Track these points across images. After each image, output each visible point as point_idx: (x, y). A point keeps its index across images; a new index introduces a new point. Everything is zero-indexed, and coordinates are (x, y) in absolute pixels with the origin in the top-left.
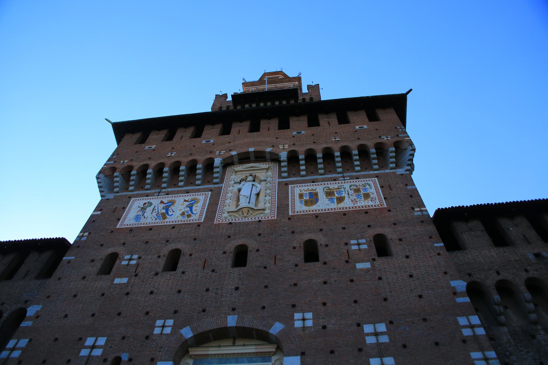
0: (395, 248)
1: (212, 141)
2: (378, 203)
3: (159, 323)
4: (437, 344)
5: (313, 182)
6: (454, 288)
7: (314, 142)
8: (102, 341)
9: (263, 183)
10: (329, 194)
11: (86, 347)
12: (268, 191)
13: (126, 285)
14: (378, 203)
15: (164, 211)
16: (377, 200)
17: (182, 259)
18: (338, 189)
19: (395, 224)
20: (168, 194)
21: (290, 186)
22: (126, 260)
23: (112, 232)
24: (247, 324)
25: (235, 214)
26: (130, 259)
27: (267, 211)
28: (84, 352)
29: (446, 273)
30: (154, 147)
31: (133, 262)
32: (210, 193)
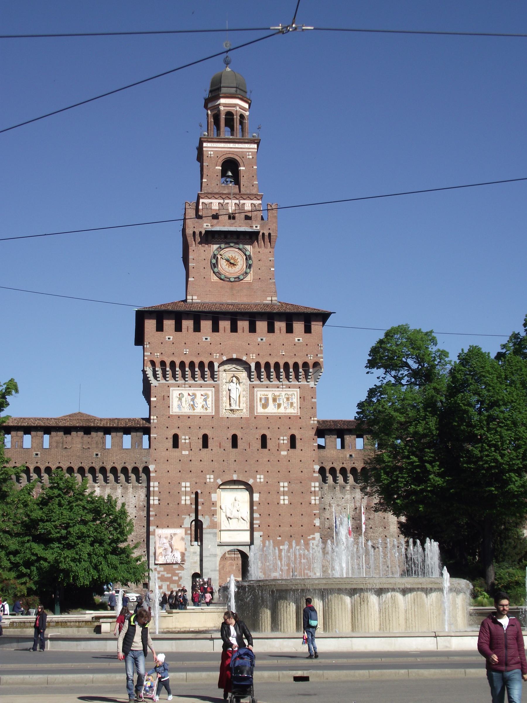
0: (298, 443)
1: (209, 340)
2: (296, 412)
3: (208, 476)
4: (302, 493)
5: (267, 387)
6: (314, 469)
7: (270, 355)
8: (188, 484)
9: (241, 384)
10: (274, 400)
11: (183, 487)
12: (244, 393)
13: (189, 455)
14: (296, 412)
15: (192, 403)
16: (296, 410)
17: (210, 441)
18: (279, 396)
19: (301, 428)
20: (190, 387)
21: (255, 389)
22: (183, 439)
23: (169, 417)
24: (240, 479)
25: (229, 411)
26: (185, 439)
27: (244, 410)
28: (183, 489)
29: (314, 461)
30: (171, 337)
31: (187, 441)
32: (214, 389)
